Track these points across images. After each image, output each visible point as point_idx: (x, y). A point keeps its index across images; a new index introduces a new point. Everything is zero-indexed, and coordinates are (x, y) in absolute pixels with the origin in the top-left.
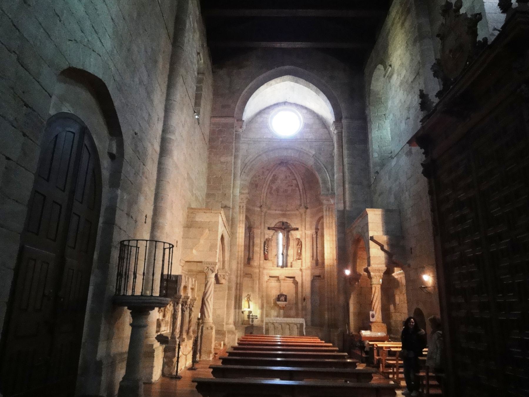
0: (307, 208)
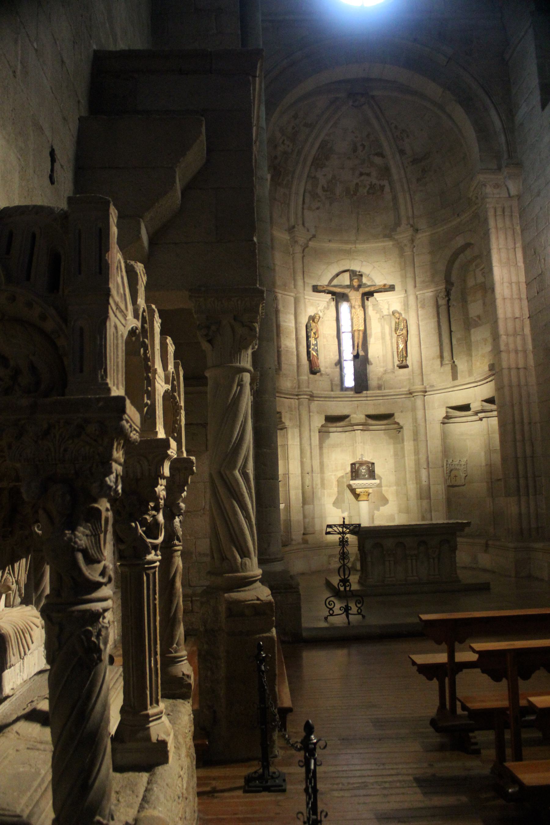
0: (417, 231)
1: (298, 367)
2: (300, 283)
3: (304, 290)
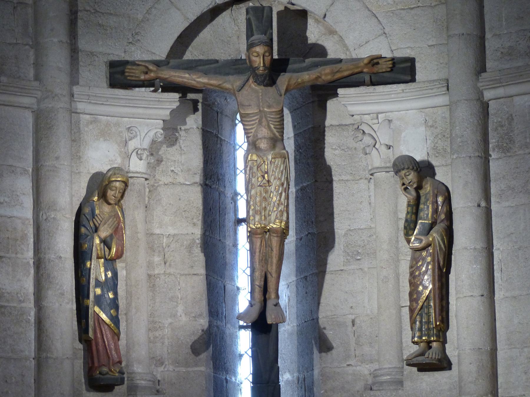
1: (41, 362)
2: (57, 57)
3: (74, 81)
